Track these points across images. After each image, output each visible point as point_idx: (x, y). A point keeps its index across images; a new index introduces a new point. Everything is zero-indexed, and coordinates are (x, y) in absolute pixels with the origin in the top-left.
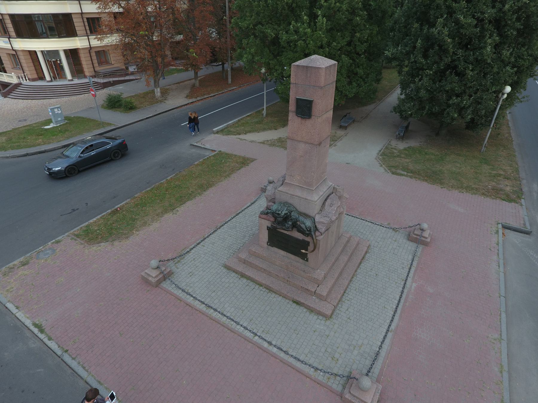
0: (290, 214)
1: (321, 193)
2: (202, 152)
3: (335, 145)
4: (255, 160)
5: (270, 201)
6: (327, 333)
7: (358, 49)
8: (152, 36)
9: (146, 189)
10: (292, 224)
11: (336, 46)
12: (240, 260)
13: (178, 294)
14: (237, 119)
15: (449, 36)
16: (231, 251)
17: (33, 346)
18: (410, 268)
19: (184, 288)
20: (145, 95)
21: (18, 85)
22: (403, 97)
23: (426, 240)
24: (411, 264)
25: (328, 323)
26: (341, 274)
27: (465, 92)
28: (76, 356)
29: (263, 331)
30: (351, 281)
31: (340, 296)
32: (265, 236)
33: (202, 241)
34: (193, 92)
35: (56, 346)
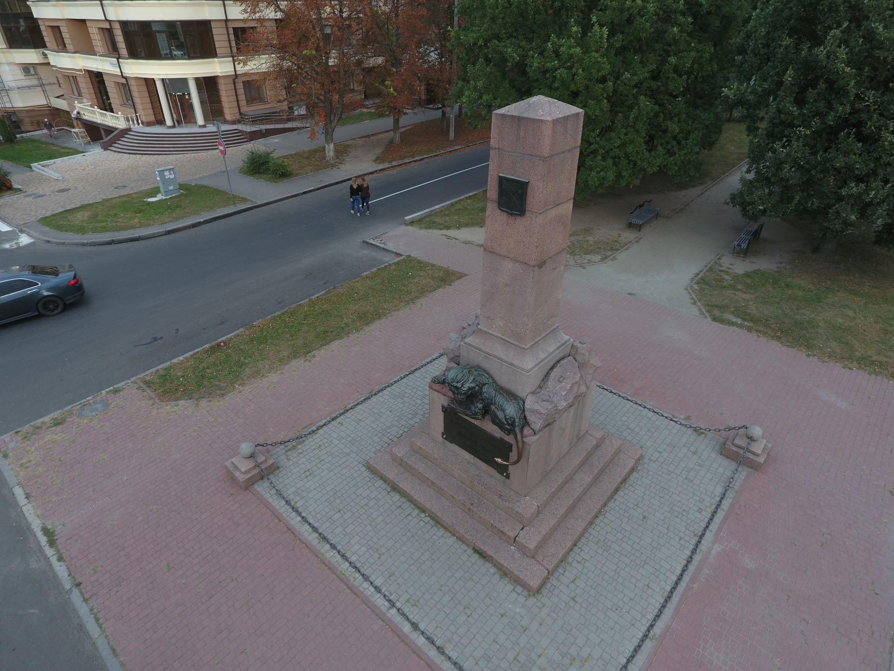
0: (481, 388)
1: (543, 356)
2: (379, 255)
3: (614, 259)
4: (465, 275)
6: (525, 623)
7: (671, 86)
8: (327, 58)
9: (275, 312)
10: (484, 407)
11: (629, 80)
12: (395, 458)
13: (277, 507)
15: (848, 63)
16: (385, 439)
17: (35, 566)
18: (715, 513)
19: (291, 497)
20: (312, 153)
21: (127, 131)
22: (751, 176)
23: (757, 459)
24: (719, 505)
25: (531, 601)
26: (573, 508)
27: (875, 173)
28: (91, 597)
29: (408, 601)
30: (591, 523)
31: (562, 553)
32: (438, 422)
33: (341, 415)
34: (390, 151)
35: (66, 574)
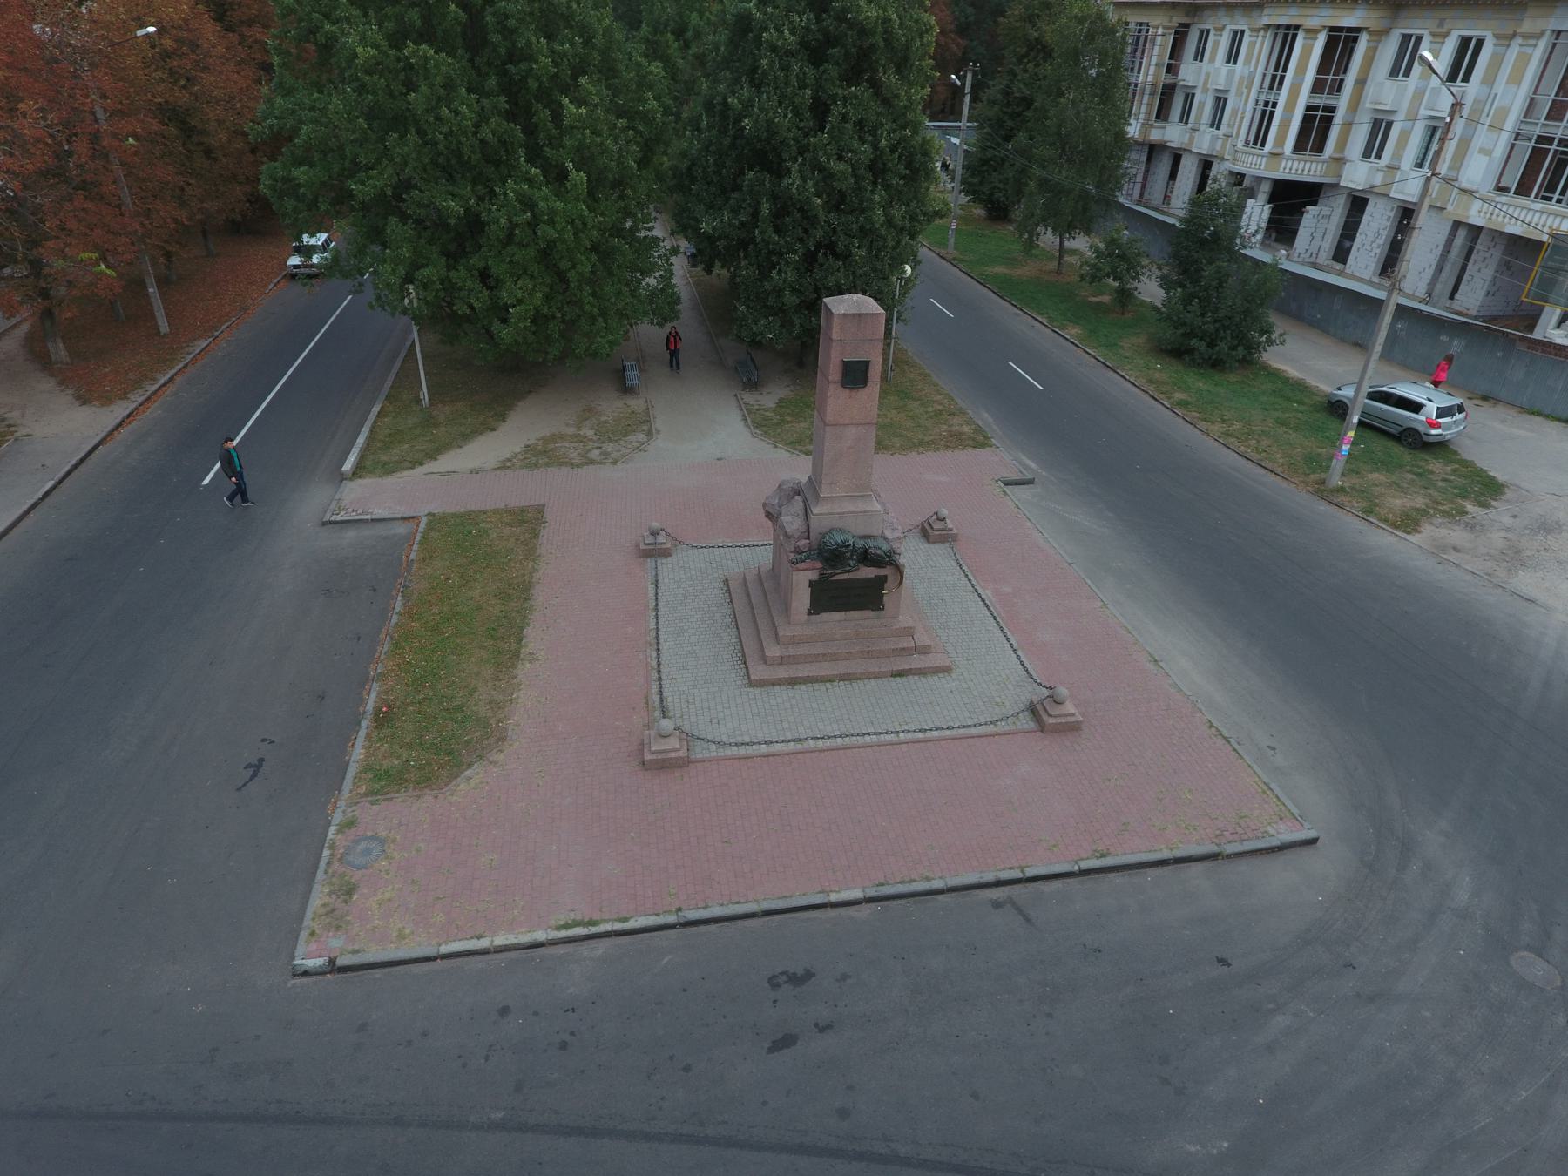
2: (381, 530)
5: (799, 539)
14: (365, 432)
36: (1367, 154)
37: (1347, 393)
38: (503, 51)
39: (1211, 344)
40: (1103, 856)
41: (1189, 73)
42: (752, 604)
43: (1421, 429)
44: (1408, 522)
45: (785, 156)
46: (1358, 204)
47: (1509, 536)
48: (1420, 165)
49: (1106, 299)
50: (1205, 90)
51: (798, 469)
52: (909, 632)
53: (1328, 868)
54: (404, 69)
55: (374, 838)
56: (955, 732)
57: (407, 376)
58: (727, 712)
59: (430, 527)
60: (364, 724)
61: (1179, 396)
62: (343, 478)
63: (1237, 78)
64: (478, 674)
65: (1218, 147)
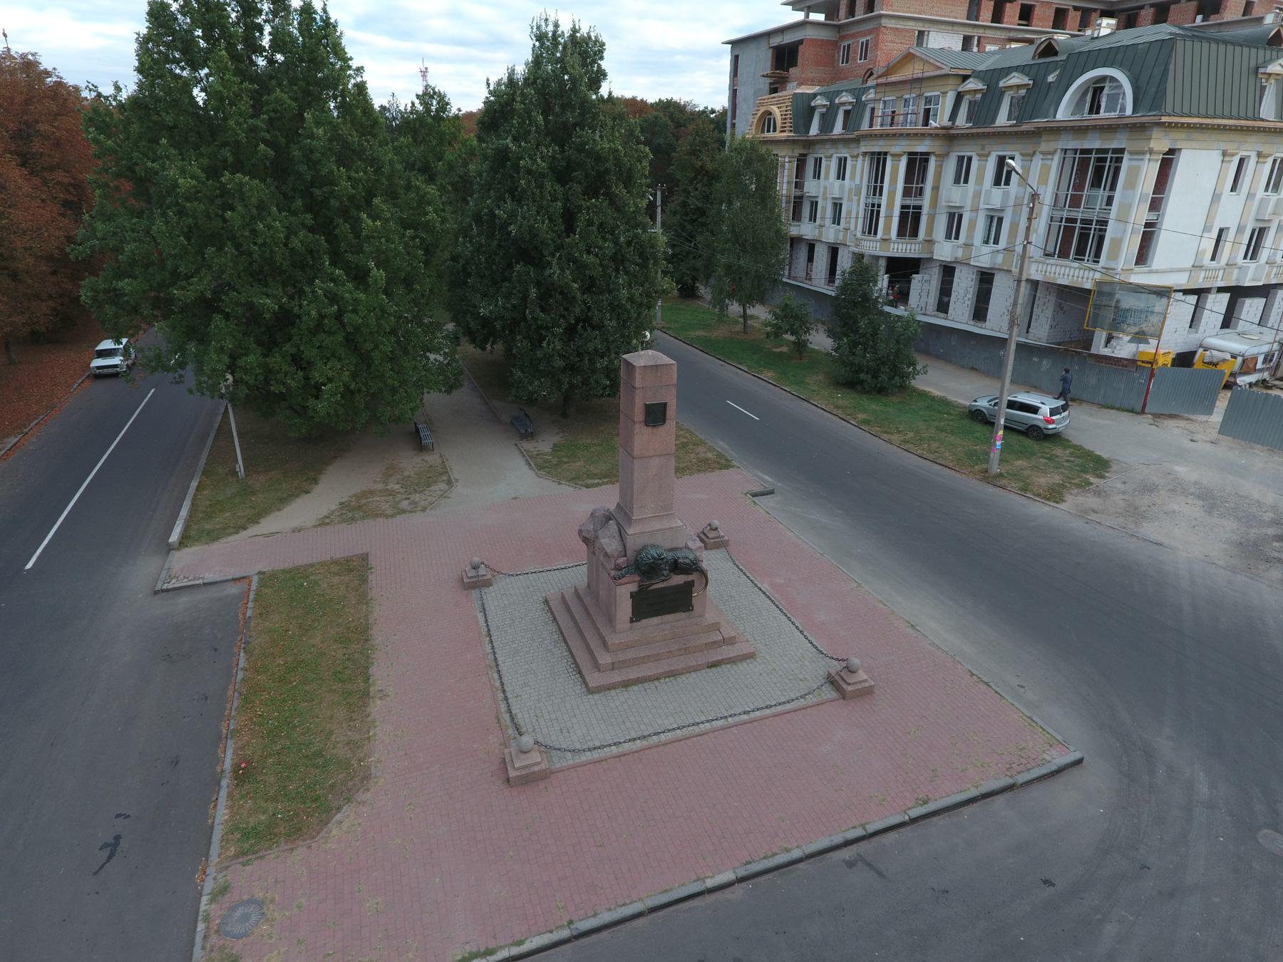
2: (214, 593)
14: (187, 505)
27: (609, 350)
36: (948, 237)
37: (983, 404)
38: (309, 178)
39: (875, 376)
40: (925, 802)
41: (811, 187)
42: (577, 621)
43: (1042, 425)
44: (1054, 495)
45: (546, 253)
46: (948, 271)
47: (1125, 497)
48: (987, 242)
49: (785, 349)
50: (825, 199)
51: (607, 497)
52: (716, 627)
53: (1098, 778)
54: (222, 196)
55: (251, 901)
56: (773, 710)
57: (221, 452)
58: (574, 720)
59: (262, 583)
60: (224, 783)
61: (861, 416)
62: (170, 548)
63: (847, 190)
64: (331, 717)
65: (841, 237)
